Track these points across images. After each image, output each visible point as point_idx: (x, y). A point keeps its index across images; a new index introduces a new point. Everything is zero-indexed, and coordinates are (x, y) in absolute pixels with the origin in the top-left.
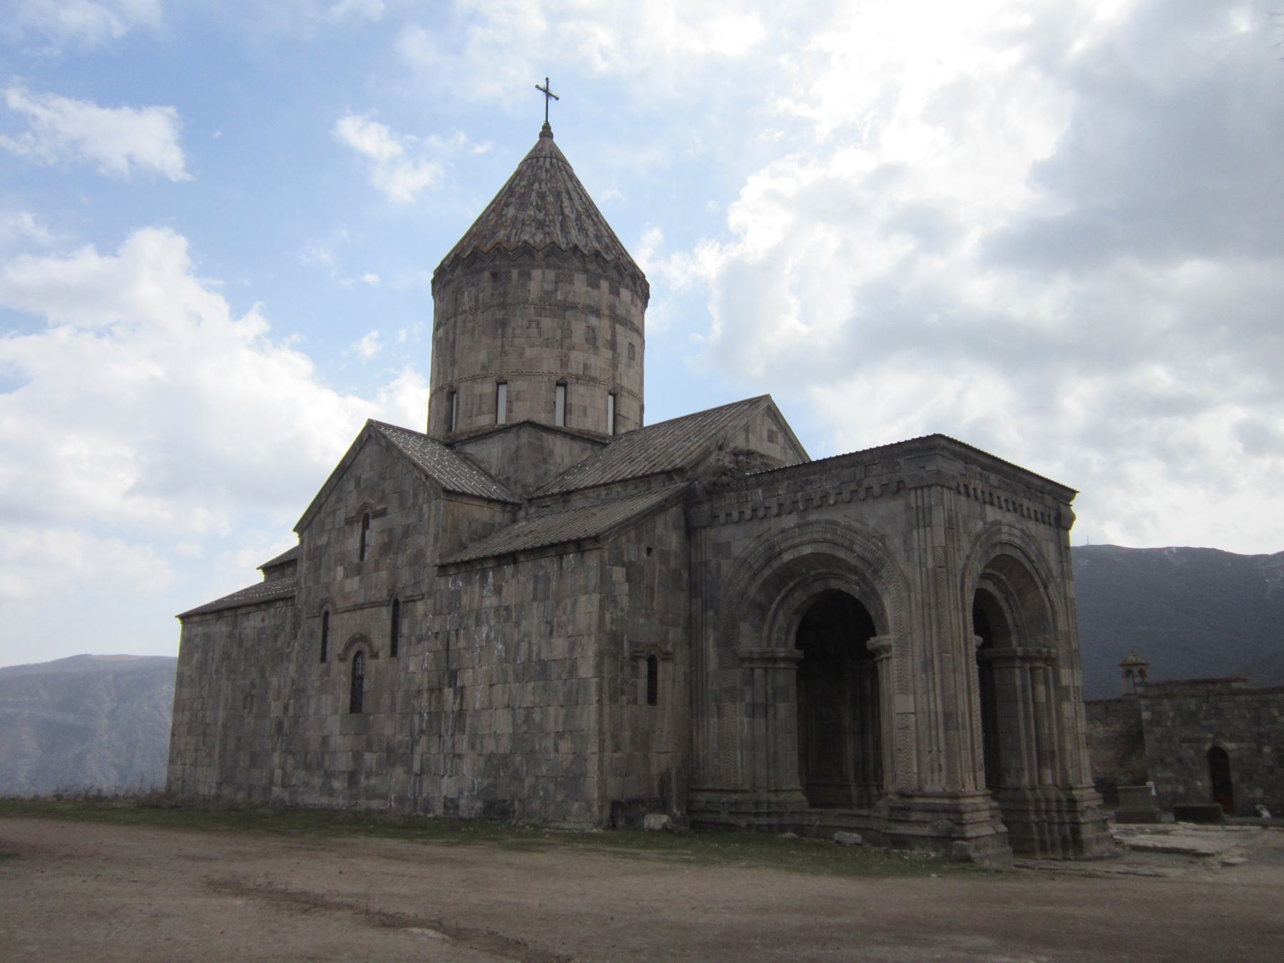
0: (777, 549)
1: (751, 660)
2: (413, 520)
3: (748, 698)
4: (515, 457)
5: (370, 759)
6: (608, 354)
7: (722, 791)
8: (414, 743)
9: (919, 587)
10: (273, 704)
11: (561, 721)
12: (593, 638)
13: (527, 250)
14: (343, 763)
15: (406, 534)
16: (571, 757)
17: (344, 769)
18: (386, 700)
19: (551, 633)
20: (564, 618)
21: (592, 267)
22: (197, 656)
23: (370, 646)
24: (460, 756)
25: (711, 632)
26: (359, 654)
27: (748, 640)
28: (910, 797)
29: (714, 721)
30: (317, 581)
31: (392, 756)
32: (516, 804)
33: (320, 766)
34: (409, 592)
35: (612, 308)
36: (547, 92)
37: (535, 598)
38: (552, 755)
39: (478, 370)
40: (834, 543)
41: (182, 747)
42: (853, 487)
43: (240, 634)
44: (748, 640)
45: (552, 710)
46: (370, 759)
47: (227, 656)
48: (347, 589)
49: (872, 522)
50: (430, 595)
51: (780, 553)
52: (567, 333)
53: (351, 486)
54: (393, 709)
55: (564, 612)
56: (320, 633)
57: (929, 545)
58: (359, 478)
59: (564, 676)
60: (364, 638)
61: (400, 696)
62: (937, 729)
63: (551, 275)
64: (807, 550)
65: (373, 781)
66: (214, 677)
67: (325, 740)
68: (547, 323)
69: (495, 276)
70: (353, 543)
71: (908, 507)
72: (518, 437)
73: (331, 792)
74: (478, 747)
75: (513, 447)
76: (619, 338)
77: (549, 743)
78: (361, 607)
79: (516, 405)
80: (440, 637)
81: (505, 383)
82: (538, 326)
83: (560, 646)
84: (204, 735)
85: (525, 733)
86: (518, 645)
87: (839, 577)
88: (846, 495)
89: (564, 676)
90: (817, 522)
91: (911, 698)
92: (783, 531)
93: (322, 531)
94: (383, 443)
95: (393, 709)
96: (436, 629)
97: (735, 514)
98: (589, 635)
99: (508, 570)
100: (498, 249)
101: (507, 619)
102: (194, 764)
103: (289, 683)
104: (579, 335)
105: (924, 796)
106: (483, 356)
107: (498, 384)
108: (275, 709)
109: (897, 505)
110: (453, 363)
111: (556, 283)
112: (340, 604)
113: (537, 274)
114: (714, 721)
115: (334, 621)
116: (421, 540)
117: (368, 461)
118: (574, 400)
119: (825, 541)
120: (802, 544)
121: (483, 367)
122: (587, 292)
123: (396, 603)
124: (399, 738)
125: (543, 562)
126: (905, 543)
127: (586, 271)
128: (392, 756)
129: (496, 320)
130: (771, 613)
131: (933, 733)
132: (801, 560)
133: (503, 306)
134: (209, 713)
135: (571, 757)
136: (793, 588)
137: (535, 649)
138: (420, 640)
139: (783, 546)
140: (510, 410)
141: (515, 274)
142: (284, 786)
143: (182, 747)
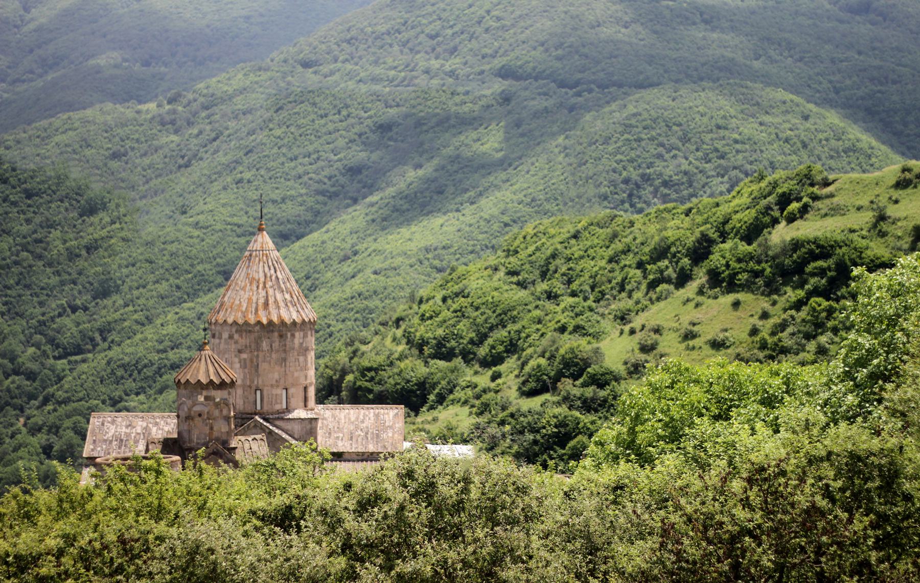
39: (274, 382)
63: (302, 333)
68: (301, 359)
69: (281, 336)
72: (311, 423)
75: (309, 427)
106: (276, 376)
110: (258, 376)
113: (297, 334)
133: (285, 351)
141: (289, 335)
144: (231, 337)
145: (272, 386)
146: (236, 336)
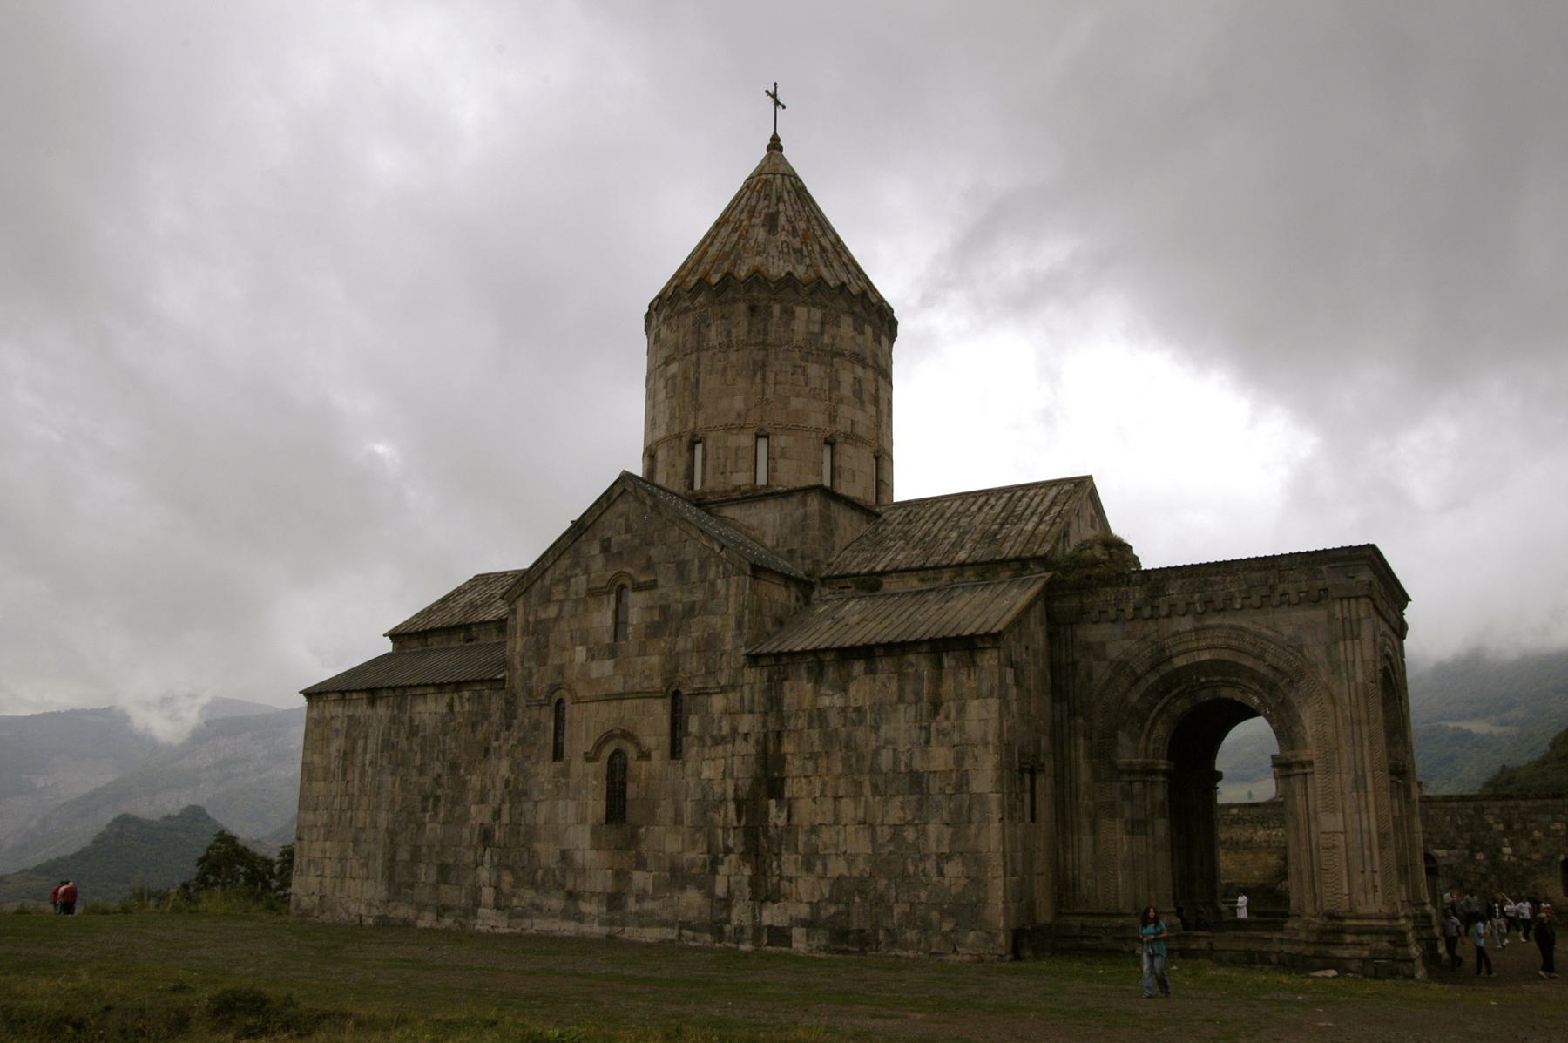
0: (1168, 653)
1: (1130, 772)
2: (698, 596)
3: (1127, 814)
4: (802, 526)
5: (641, 879)
6: (871, 410)
7: (1099, 915)
8: (715, 863)
9: (1347, 700)
10: (474, 809)
11: (946, 842)
12: (991, 748)
13: (789, 280)
14: (601, 881)
15: (690, 611)
16: (963, 881)
17: (599, 889)
18: (665, 811)
19: (928, 742)
20: (945, 724)
21: (858, 309)
22: (337, 744)
23: (638, 745)
24: (790, 879)
25: (1081, 741)
26: (617, 753)
27: (1127, 752)
28: (1341, 918)
29: (1087, 839)
30: (542, 662)
31: (678, 877)
32: (882, 935)
33: (562, 886)
34: (697, 684)
35: (875, 356)
36: (774, 96)
37: (901, 699)
38: (935, 879)
39: (732, 419)
40: (1240, 651)
41: (318, 855)
42: (1265, 591)
43: (411, 720)
44: (1127, 752)
45: (932, 829)
46: (641, 879)
47: (387, 745)
48: (594, 674)
49: (1288, 631)
50: (733, 687)
51: (1171, 657)
52: (835, 384)
53: (595, 549)
54: (678, 820)
55: (947, 717)
56: (552, 725)
57: (1358, 658)
58: (609, 539)
59: (949, 790)
60: (628, 735)
61: (688, 808)
62: (1370, 848)
63: (817, 314)
64: (1206, 656)
65: (649, 905)
66: (370, 771)
67: (565, 856)
68: (814, 370)
69: (753, 309)
70: (602, 618)
71: (1331, 617)
72: (804, 504)
73: (579, 917)
74: (819, 868)
76: (881, 393)
77: (930, 866)
78: (620, 697)
79: (782, 465)
80: (752, 740)
81: (767, 437)
82: (804, 373)
83: (940, 757)
84: (356, 841)
85: (890, 853)
86: (876, 753)
87: (1234, 685)
88: (1255, 600)
89: (949, 790)
90: (1220, 626)
91: (1340, 815)
92: (1176, 634)
93: (547, 599)
94: (649, 502)
95: (678, 820)
96: (743, 728)
97: (1112, 613)
98: (986, 744)
99: (858, 667)
100: (756, 279)
101: (861, 722)
102: (341, 876)
103: (499, 785)
104: (846, 390)
105: (1359, 918)
106: (738, 403)
107: (758, 436)
108: (479, 815)
109: (1319, 615)
110: (698, 407)
111: (823, 324)
112: (581, 690)
113: (801, 312)
114: (1087, 839)
115: (572, 712)
116: (716, 621)
117: (622, 521)
118: (843, 461)
119: (1229, 647)
120: (1199, 649)
121: (739, 415)
122: (853, 338)
123: (677, 693)
124: (690, 855)
125: (912, 658)
126: (1329, 654)
127: (853, 313)
128: (678, 877)
129: (755, 362)
130: (1149, 723)
131: (1367, 852)
132: (1199, 667)
133: (764, 346)
134: (361, 815)
135: (963, 881)
136: (1177, 696)
137: (904, 758)
138: (718, 741)
139: (1174, 650)
140: (771, 471)
141: (776, 309)
142: (497, 907)
143: (318, 855)
144: (657, 337)
145: (727, 428)
146: (664, 331)
